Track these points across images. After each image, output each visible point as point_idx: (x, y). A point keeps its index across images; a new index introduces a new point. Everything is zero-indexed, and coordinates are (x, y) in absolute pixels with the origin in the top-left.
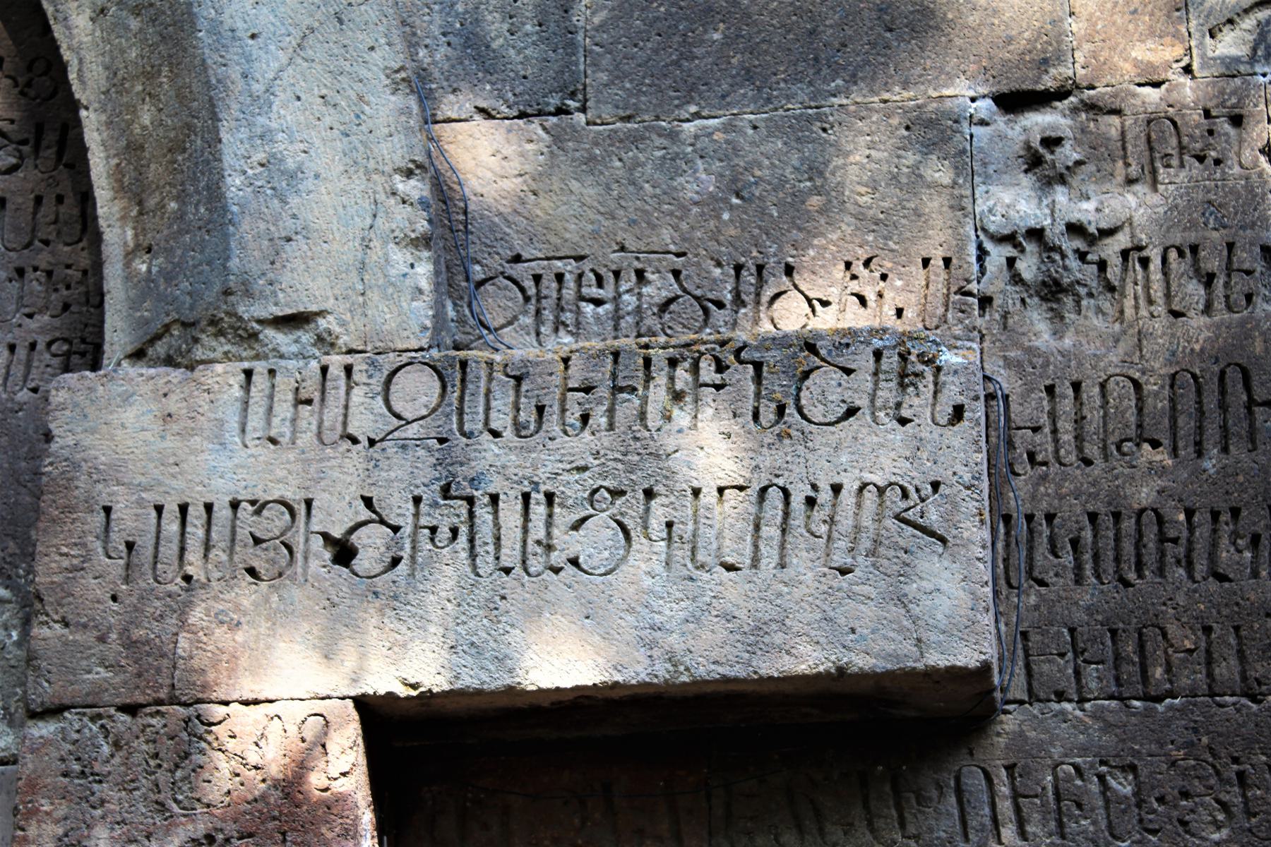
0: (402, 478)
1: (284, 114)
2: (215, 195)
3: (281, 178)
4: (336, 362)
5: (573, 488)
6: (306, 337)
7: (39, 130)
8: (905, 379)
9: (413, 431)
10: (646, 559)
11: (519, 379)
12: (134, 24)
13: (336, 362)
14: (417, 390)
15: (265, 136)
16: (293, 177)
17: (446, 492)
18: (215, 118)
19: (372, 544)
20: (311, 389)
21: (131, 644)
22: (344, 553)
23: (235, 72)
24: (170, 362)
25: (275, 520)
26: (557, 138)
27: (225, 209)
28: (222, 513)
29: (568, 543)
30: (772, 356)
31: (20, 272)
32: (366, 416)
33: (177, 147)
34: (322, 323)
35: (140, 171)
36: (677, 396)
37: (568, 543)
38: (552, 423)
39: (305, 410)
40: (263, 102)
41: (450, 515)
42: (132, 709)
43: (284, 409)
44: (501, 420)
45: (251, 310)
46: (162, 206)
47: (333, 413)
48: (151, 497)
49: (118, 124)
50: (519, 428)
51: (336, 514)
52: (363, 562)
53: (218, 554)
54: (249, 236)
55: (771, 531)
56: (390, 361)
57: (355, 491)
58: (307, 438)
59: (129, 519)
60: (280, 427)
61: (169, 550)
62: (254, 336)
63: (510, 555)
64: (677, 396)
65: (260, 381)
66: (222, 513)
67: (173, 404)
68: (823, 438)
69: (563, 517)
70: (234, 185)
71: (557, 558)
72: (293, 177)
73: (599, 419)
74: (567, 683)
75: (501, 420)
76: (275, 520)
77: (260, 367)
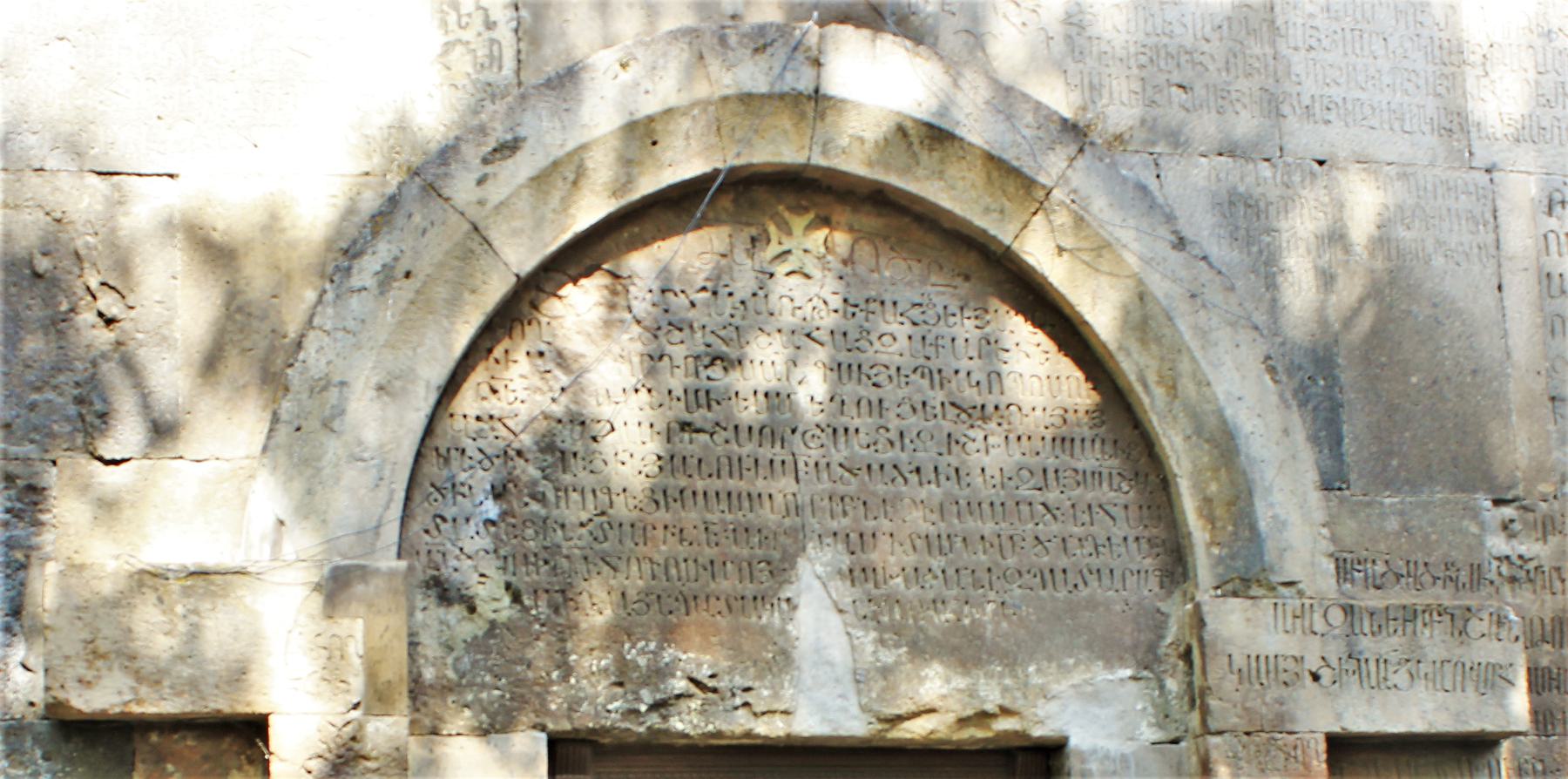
0: (1335, 650)
1: (1277, 497)
2: (1253, 527)
3: (1280, 524)
4: (1307, 602)
5: (1393, 657)
6: (1293, 590)
7: (1137, 474)
8: (1500, 623)
9: (1337, 632)
10: (1421, 685)
11: (1372, 614)
12: (1206, 446)
13: (1307, 602)
14: (1337, 616)
15: (1271, 505)
16: (1284, 523)
17: (1350, 657)
18: (1250, 494)
19: (1326, 674)
20: (1298, 613)
21: (1246, 709)
22: (1316, 677)
23: (1257, 476)
24: (1235, 594)
25: (1291, 665)
26: (1342, 501)
27: (1259, 535)
28: (1272, 660)
29: (1394, 679)
30: (1457, 612)
31: (1137, 539)
32: (1319, 626)
33: (1231, 504)
34: (1301, 586)
35: (1211, 510)
36: (1425, 625)
37: (1394, 679)
38: (1384, 633)
39: (1298, 621)
40: (1269, 490)
41: (1352, 665)
42: (1248, 734)
43: (1290, 620)
44: (1367, 630)
45: (1275, 579)
46: (1224, 528)
47: (1307, 624)
48: (1247, 652)
49: (1198, 487)
50: (1373, 634)
51: (1313, 663)
52: (1325, 680)
53: (1272, 675)
54: (1270, 547)
55: (1459, 678)
56: (1327, 603)
57: (1318, 654)
58: (1299, 632)
59: (1239, 661)
60: (1289, 628)
61: (1254, 673)
62: (1274, 589)
63: (1374, 683)
64: (1425, 625)
65: (1280, 608)
66: (1272, 660)
67: (1249, 614)
68: (1476, 644)
69: (1391, 669)
70: (1263, 525)
71: (1389, 683)
72: (1284, 523)
73: (1400, 632)
74: (1395, 730)
75: (1367, 630)
76: (1291, 665)
77: (1280, 602)
